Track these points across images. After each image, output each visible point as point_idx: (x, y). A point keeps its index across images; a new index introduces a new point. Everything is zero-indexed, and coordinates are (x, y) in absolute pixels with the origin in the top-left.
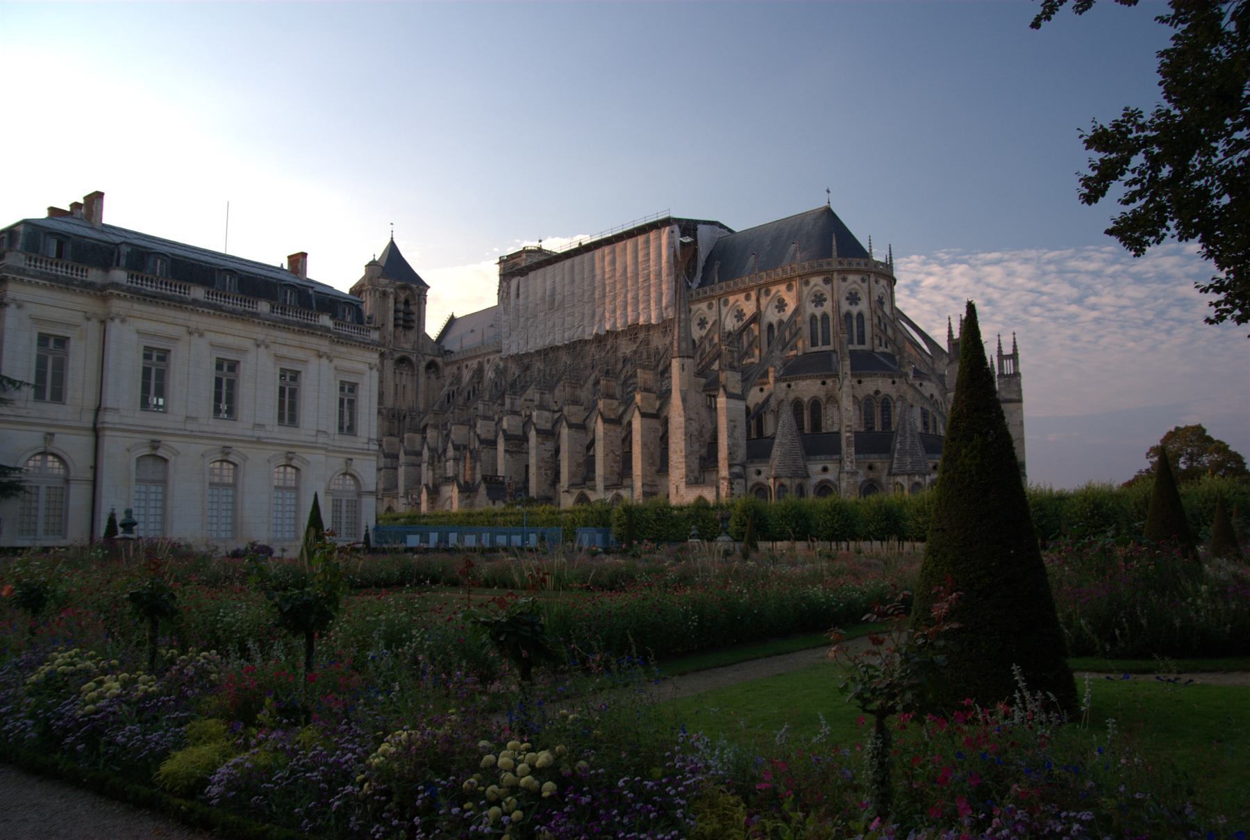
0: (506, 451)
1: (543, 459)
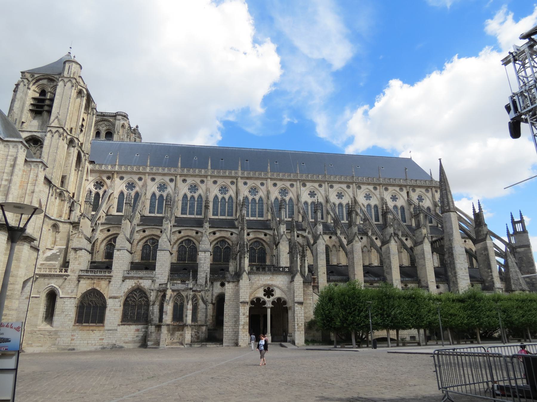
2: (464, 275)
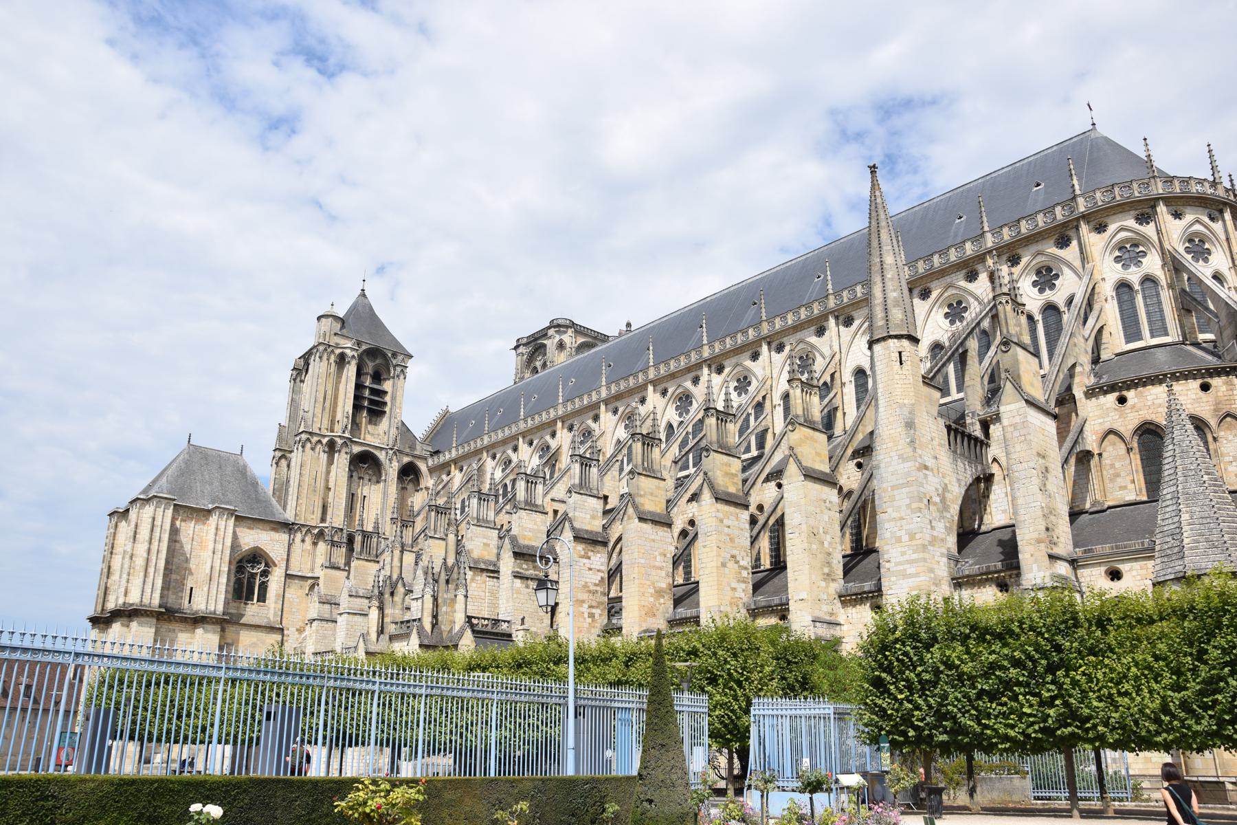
1: (586, 586)
2: (906, 557)
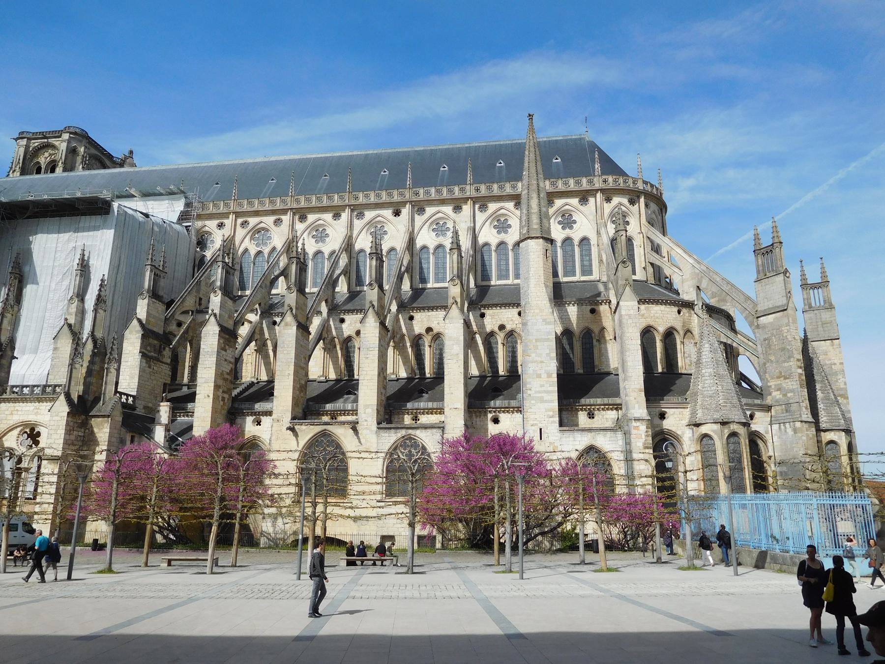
0: (144, 355)
1: (222, 374)
